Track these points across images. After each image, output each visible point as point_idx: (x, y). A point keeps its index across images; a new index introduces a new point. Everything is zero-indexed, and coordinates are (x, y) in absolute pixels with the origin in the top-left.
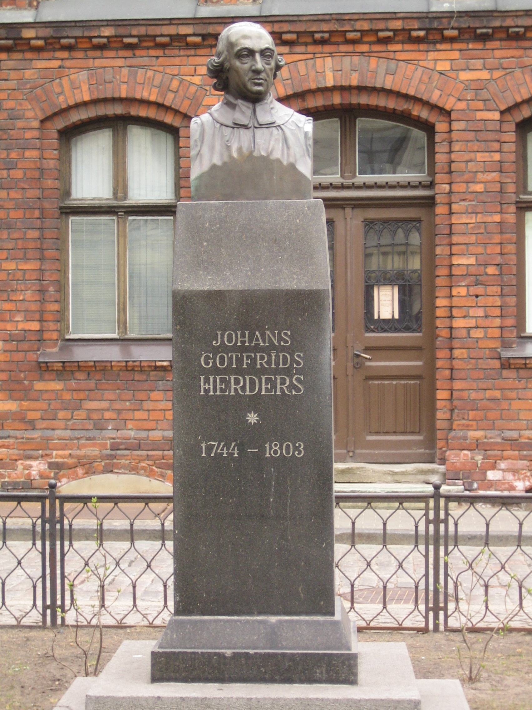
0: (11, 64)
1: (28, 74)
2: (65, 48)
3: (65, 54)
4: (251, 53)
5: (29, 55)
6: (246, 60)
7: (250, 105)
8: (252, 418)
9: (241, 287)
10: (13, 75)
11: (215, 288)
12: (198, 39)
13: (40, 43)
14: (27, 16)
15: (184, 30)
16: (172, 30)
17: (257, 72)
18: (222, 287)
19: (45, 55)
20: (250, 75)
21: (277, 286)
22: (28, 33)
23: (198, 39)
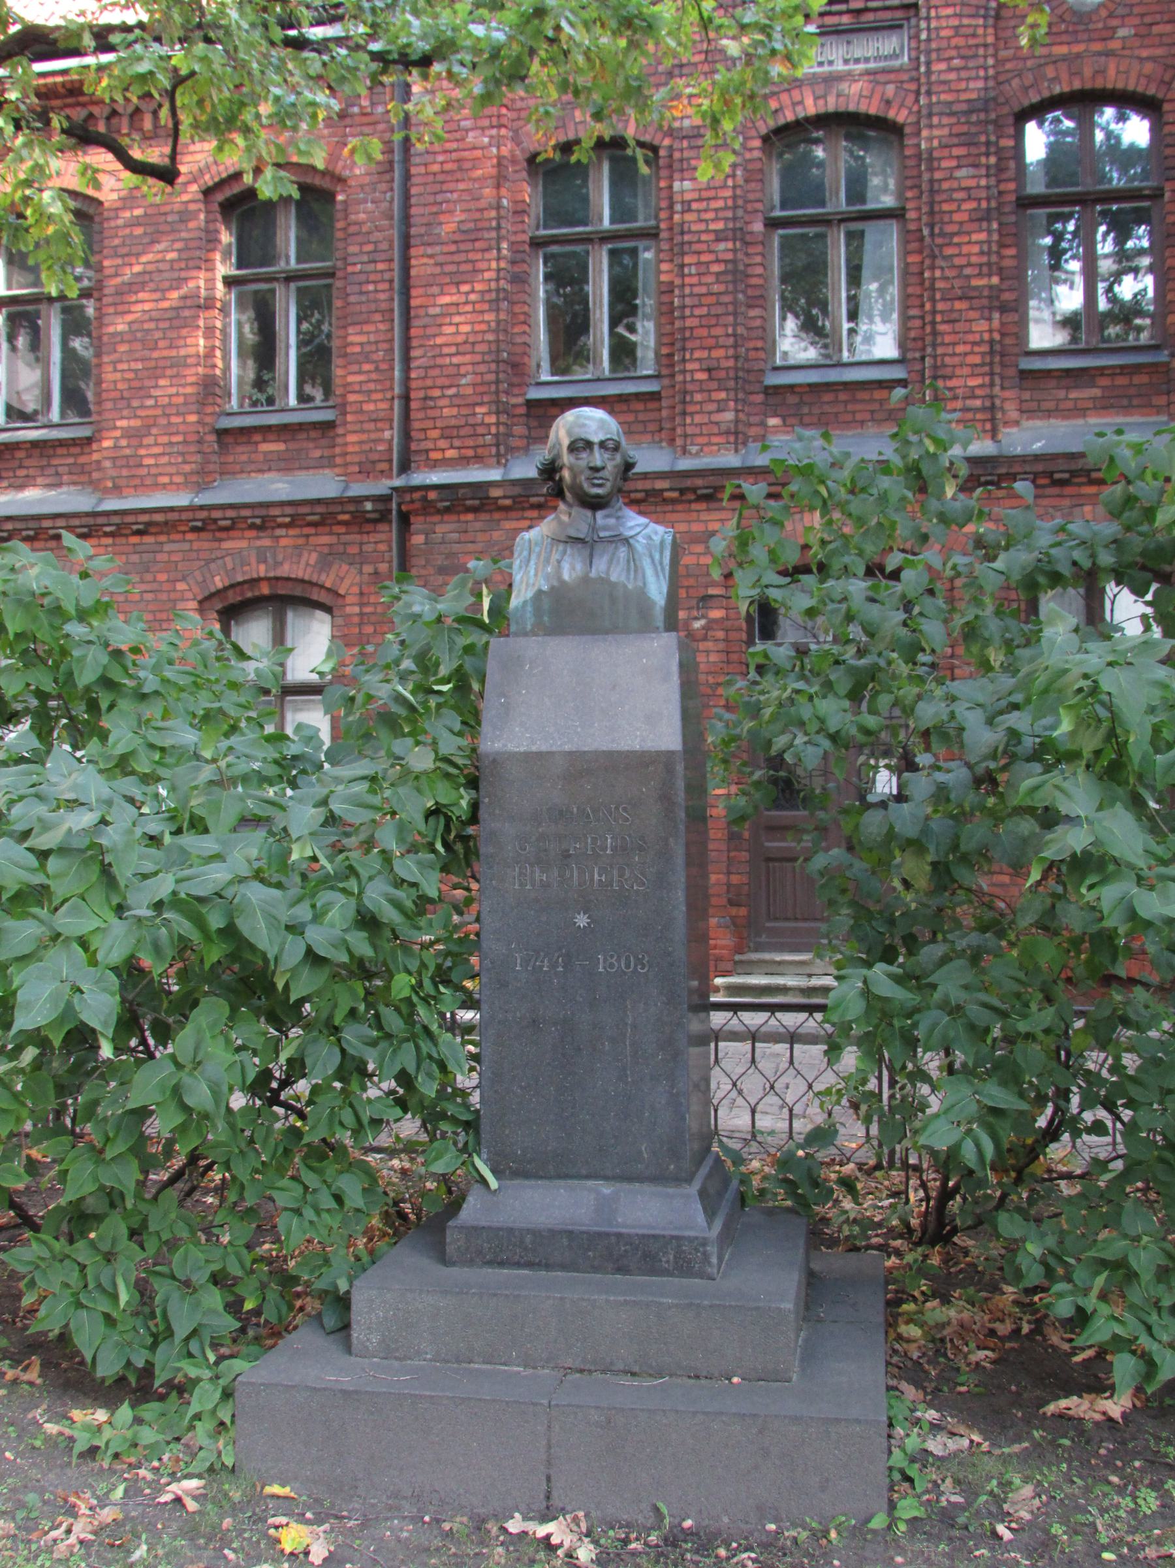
0: (478, 525)
1: (496, 535)
2: (534, 507)
3: (535, 514)
4: (589, 445)
5: (497, 516)
6: (584, 455)
7: (589, 513)
8: (582, 921)
9: (567, 748)
10: (480, 537)
11: (534, 749)
12: (675, 494)
13: (508, 502)
14: (495, 475)
15: (660, 485)
16: (648, 485)
17: (596, 469)
18: (544, 748)
19: (513, 514)
20: (588, 473)
21: (614, 747)
22: (495, 493)
23: (675, 494)
